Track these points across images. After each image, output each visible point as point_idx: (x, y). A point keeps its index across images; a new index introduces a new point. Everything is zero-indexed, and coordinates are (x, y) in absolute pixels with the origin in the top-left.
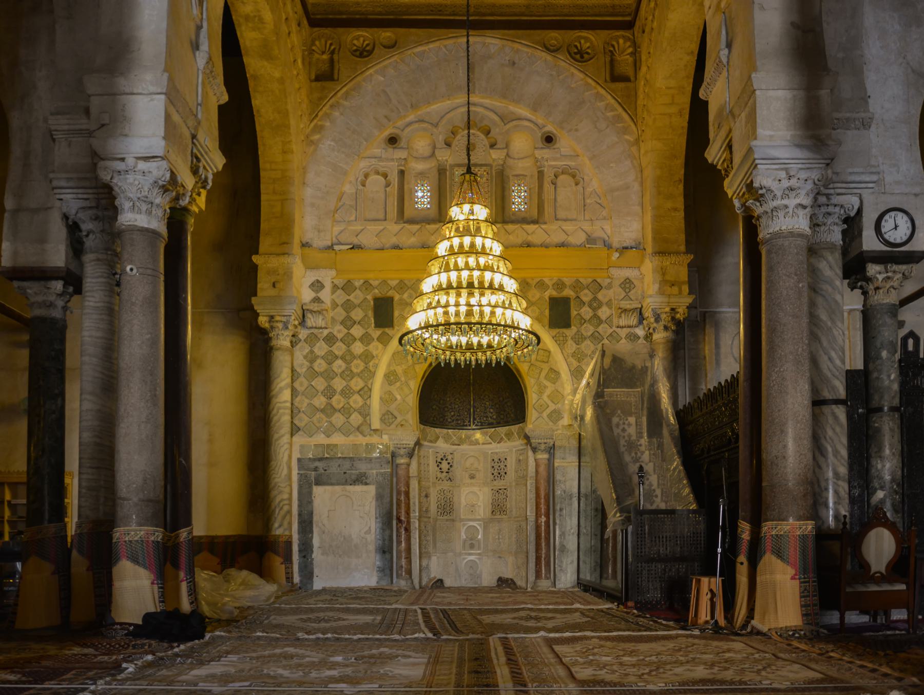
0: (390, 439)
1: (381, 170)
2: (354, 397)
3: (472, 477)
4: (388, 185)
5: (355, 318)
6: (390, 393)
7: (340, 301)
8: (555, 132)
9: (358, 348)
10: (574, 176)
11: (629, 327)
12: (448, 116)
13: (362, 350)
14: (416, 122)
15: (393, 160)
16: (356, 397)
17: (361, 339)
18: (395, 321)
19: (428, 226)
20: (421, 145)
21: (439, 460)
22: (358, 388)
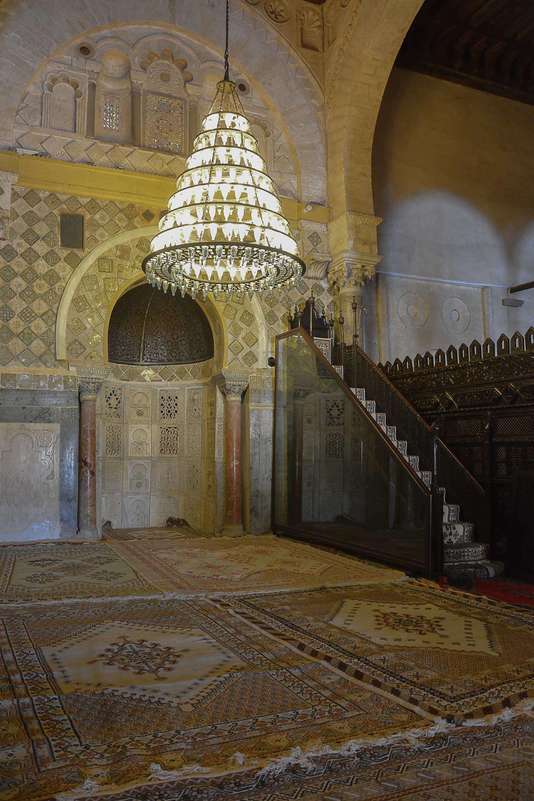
0: (78, 372)
1: (71, 78)
2: (36, 322)
3: (140, 414)
4: (78, 95)
5: (39, 233)
6: (79, 321)
7: (21, 211)
8: (248, 81)
9: (41, 266)
10: (265, 128)
11: (316, 278)
12: (145, 40)
13: (46, 270)
14: (111, 37)
15: (84, 71)
16: (39, 321)
17: (45, 257)
18: (86, 242)
19: (121, 147)
20: (113, 64)
21: (109, 396)
22: (42, 312)
